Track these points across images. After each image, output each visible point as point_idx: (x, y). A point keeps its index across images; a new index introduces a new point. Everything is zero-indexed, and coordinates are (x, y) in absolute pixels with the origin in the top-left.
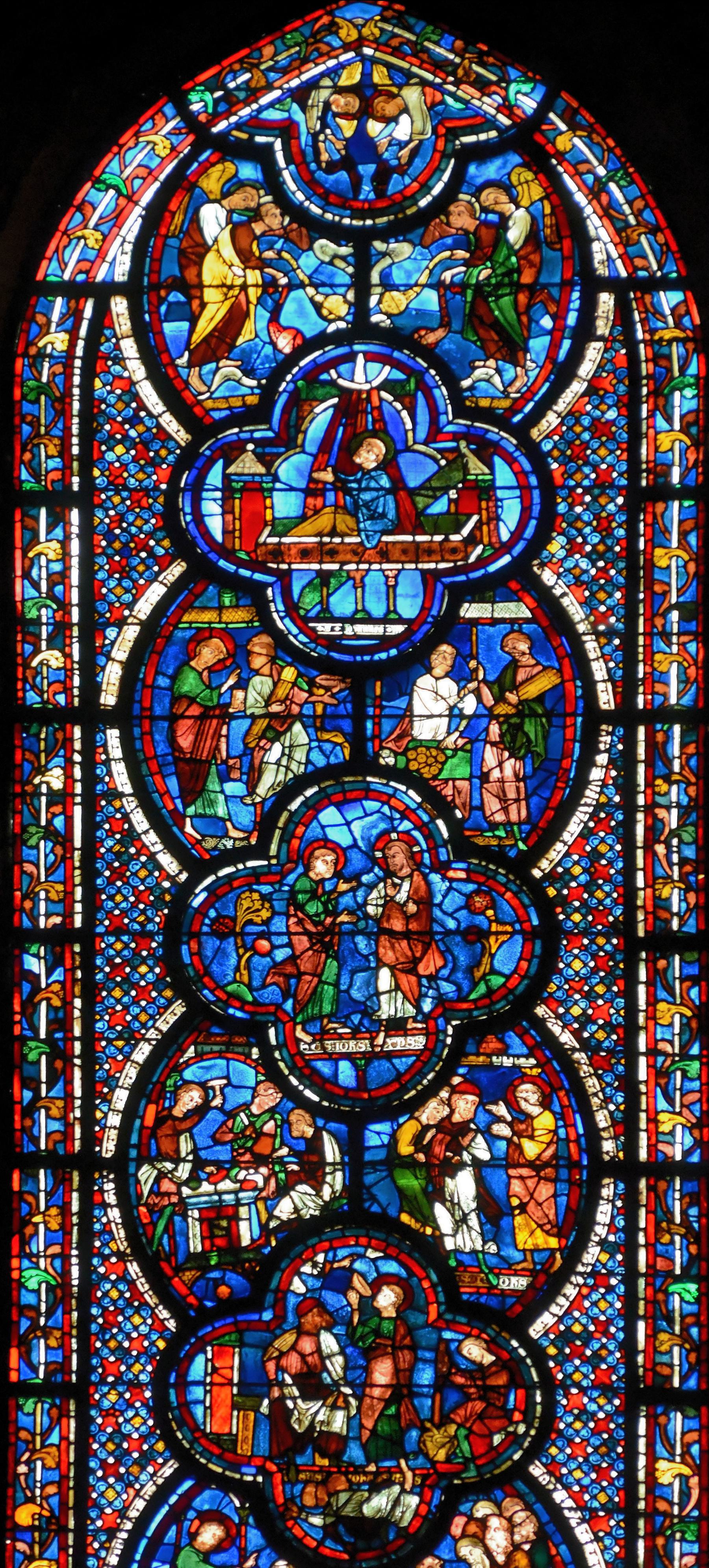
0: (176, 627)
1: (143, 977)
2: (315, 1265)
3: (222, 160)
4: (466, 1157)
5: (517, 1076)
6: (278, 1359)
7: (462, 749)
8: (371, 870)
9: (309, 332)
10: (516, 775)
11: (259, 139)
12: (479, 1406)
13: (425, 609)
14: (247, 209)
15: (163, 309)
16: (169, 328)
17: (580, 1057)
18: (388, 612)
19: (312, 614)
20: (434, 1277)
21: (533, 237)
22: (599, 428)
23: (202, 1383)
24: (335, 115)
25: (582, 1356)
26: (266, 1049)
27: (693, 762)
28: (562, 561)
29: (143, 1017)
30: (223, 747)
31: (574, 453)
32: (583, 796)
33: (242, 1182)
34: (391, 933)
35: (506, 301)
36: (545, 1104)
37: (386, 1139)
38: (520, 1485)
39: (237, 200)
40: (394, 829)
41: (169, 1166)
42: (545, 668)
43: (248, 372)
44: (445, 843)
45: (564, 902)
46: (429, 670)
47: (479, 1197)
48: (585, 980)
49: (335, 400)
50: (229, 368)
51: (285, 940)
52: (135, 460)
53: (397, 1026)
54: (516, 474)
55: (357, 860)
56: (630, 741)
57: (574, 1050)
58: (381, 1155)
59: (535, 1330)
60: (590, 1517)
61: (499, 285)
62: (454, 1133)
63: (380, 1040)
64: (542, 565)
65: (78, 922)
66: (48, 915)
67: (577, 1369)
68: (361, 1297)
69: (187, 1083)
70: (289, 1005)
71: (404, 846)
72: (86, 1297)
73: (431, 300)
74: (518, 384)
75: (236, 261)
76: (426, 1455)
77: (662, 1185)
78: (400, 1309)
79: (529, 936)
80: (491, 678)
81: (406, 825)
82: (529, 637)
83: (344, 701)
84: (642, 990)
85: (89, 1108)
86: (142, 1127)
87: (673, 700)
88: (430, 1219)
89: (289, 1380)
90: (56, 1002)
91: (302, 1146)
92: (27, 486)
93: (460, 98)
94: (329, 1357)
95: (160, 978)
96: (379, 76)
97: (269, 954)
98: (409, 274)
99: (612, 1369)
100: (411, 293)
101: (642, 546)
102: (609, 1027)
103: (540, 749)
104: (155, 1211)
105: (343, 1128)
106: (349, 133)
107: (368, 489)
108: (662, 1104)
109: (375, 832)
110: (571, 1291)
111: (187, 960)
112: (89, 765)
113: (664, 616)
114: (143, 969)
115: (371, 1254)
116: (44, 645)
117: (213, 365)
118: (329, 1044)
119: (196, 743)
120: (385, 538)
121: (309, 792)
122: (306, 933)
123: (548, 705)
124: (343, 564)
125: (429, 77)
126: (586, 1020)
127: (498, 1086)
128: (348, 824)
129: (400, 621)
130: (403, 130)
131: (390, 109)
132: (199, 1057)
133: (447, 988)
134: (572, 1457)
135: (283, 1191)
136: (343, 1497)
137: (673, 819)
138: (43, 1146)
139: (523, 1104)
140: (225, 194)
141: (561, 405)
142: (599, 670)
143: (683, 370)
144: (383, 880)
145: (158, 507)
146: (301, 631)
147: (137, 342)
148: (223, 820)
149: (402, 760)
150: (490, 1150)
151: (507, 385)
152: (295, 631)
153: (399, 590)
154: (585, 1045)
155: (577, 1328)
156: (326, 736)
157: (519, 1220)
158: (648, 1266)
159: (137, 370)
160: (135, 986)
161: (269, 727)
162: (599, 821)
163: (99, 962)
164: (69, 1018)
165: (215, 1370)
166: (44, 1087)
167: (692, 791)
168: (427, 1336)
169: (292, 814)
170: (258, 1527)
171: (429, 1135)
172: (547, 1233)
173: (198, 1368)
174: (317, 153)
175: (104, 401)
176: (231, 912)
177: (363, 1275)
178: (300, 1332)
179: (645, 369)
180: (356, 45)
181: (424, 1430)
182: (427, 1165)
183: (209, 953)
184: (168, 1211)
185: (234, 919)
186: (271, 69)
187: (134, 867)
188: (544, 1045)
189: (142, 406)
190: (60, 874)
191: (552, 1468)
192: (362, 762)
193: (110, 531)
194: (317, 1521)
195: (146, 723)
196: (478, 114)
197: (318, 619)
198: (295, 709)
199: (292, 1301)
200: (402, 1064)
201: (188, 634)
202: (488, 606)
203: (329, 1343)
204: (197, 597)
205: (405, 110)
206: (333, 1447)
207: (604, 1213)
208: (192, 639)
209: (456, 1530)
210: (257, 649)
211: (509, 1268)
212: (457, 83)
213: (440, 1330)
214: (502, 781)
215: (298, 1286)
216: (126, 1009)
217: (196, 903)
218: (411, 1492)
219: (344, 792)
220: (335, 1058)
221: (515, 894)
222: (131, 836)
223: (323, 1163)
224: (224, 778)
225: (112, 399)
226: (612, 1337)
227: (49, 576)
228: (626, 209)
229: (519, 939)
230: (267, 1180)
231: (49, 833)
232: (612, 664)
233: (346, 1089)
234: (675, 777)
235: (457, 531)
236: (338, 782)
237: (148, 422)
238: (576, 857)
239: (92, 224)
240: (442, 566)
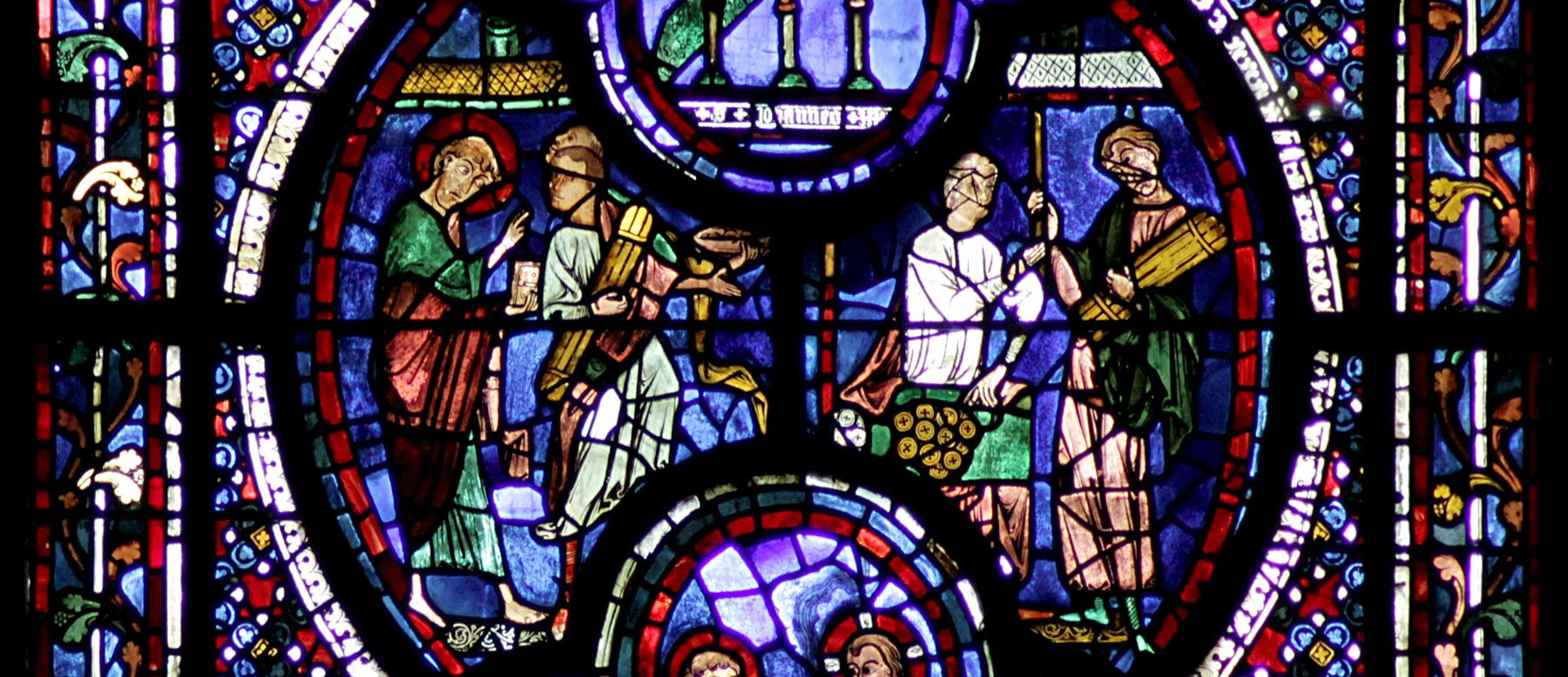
0: (390, 109)
7: (1013, 408)
10: (1130, 472)
13: (931, 67)
18: (851, 74)
19: (684, 78)
27: (1516, 443)
40: (866, 604)
42: (1192, 212)
56: (1378, 391)
71: (887, 646)
80: (1075, 235)
81: (892, 595)
82: (1157, 135)
83: (754, 291)
109: (824, 610)
112: (197, 445)
113: (1450, 85)
119: (432, 391)
121: (680, 514)
128: (766, 590)
146: (662, 121)
148: (493, 580)
149: (882, 433)
152: (648, 120)
156: (717, 377)
161: (592, 352)
162: (1311, 588)
167: (1514, 511)
169: (644, 565)
192: (797, 441)
195: (325, 339)
197: (698, 91)
198: (650, 308)
201: (415, 124)
202: (1068, 59)
204: (435, 34)
210: (565, 163)
214: (1099, 486)
219: (756, 512)
222: (292, 619)
224: (495, 477)
231: (113, 612)
232: (1337, 204)
234: (1480, 480)
236: (741, 491)
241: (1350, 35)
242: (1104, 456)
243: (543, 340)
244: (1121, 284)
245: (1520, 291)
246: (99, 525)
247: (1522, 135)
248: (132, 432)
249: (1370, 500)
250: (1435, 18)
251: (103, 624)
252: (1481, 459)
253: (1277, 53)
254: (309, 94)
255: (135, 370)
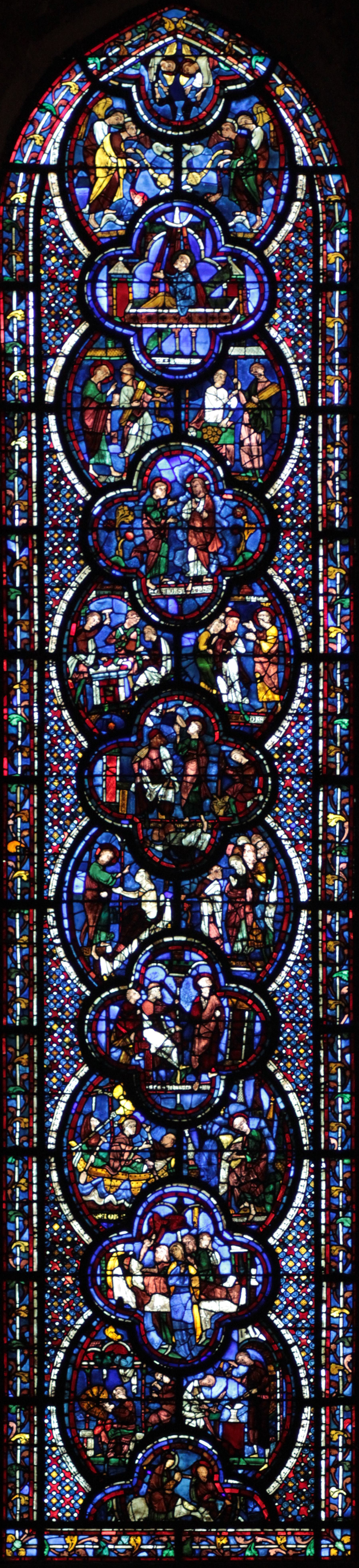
1: (69, 553)
2: (157, 711)
3: (105, 97)
4: (233, 651)
5: (258, 607)
6: (139, 762)
7: (230, 427)
8: (183, 494)
9: (151, 195)
10: (257, 442)
11: (124, 85)
12: (240, 786)
13: (211, 350)
14: (118, 125)
15: (75, 180)
16: (79, 191)
17: (290, 596)
20: (217, 717)
21: (264, 142)
22: (298, 250)
23: (101, 775)
24: (164, 72)
25: (291, 759)
26: (132, 593)
27: (346, 435)
28: (280, 324)
29: (69, 576)
30: (109, 425)
31: (285, 264)
32: (290, 454)
33: (121, 665)
34: (195, 529)
35: (251, 178)
36: (272, 622)
37: (193, 642)
38: (261, 828)
39: (113, 120)
40: (196, 472)
41: (83, 657)
42: (272, 384)
43: (120, 217)
44: (222, 479)
45: (282, 512)
46: (213, 384)
47: (240, 673)
48: (292, 555)
49: (164, 233)
50: (110, 214)
51: (141, 532)
52: (62, 265)
53: (198, 580)
54: (257, 275)
55: (177, 489)
56: (314, 424)
57: (287, 593)
58: (190, 651)
59: (268, 745)
60: (295, 845)
61: (248, 170)
62: (227, 638)
63: (189, 588)
64: (270, 326)
65: (35, 522)
66: (20, 519)
67: (289, 766)
68: (181, 728)
69: (92, 612)
70: (143, 569)
72: (42, 729)
73: (213, 177)
74: (257, 225)
75: (113, 154)
76: (214, 813)
77: (331, 666)
78: (200, 733)
79: (265, 530)
80: (245, 388)
81: (202, 469)
82: (263, 366)
83: (169, 401)
84: (321, 560)
85: (42, 626)
86: (69, 636)
87: (336, 401)
88: (215, 686)
89: (144, 773)
90: (25, 567)
91: (150, 646)
92: (6, 279)
93: (227, 63)
94: (165, 760)
95: (77, 554)
96: (186, 50)
97: (133, 540)
98: (201, 163)
99: (306, 766)
100: (203, 174)
101: (320, 316)
102: (305, 581)
103: (269, 428)
104: (76, 682)
105: (171, 636)
106: (170, 83)
107: (182, 282)
108: (331, 622)
109: (186, 473)
110: (286, 724)
111: (91, 544)
112: (40, 435)
114: (69, 549)
115: (186, 705)
116: (16, 368)
117: (101, 213)
118: (163, 590)
120: (190, 310)
121: (153, 451)
122: (151, 528)
123: (273, 403)
124: (169, 324)
125: (211, 52)
126: (293, 577)
127: (248, 613)
128: (172, 468)
129: (198, 357)
130: (198, 82)
131: (191, 69)
132: (98, 597)
133: (223, 559)
134: (286, 813)
135: (141, 670)
136: (172, 836)
137: (336, 466)
138: (19, 646)
139: (262, 623)
140: (107, 116)
141: (280, 237)
142: (299, 384)
143: (341, 218)
144: (190, 499)
145: (74, 292)
147: (63, 199)
149: (200, 433)
150: (245, 647)
151: (252, 225)
152: (145, 361)
153: (198, 339)
154: (293, 590)
155: (289, 744)
157: (260, 685)
158: (324, 710)
159: (62, 214)
160: (65, 558)
161: (132, 415)
162: (299, 468)
163: (46, 545)
164: (32, 576)
165: (108, 768)
166: (19, 614)
167: (346, 451)
168: (214, 749)
169: (144, 463)
170: (130, 851)
171: (214, 640)
172: (274, 693)
173: (99, 767)
174: (154, 94)
175: (45, 232)
176: (113, 517)
177: (182, 716)
178: (151, 747)
179: (321, 217)
180: (173, 33)
181: (212, 800)
182: (214, 656)
183: (102, 540)
184: (83, 682)
185: (115, 521)
186: (129, 46)
187: (64, 492)
188: (272, 590)
189: (65, 235)
190: (25, 496)
191: (276, 819)
192: (180, 435)
193: (49, 305)
194: (159, 848)
195: (69, 412)
196: (236, 73)
198: (145, 405)
199: (146, 730)
200: (200, 601)
201: (90, 363)
202: (243, 349)
203: (165, 753)
204: (95, 342)
205: (199, 70)
206: (167, 809)
207: (302, 681)
208: (92, 366)
209: (229, 852)
211: (254, 712)
212: (225, 56)
213: (220, 745)
214: (250, 445)
215: (149, 722)
216: (60, 571)
217: (96, 512)
218: (207, 833)
219: (170, 451)
220: (167, 598)
221: (257, 508)
222: (62, 475)
223: (161, 655)
224: (109, 443)
225: (49, 231)
226: (306, 748)
227: (19, 329)
228: (312, 128)
229: (259, 532)
230: (133, 664)
231: (20, 473)
233: (173, 615)
235: (227, 307)
236: (166, 446)
237: (69, 244)
238: (287, 488)
239: (38, 131)
240: (219, 326)
241: (308, 343)
242: (251, 438)
243: (119, 413)
244: (255, 399)
245: (347, 401)
246: (17, 454)
247: (348, 366)
248: (23, 432)
249: (312, 448)
250: (328, 340)
251: (18, 476)
252: (338, 439)
253: (291, 347)
254: (65, 356)
255: (25, 418)
